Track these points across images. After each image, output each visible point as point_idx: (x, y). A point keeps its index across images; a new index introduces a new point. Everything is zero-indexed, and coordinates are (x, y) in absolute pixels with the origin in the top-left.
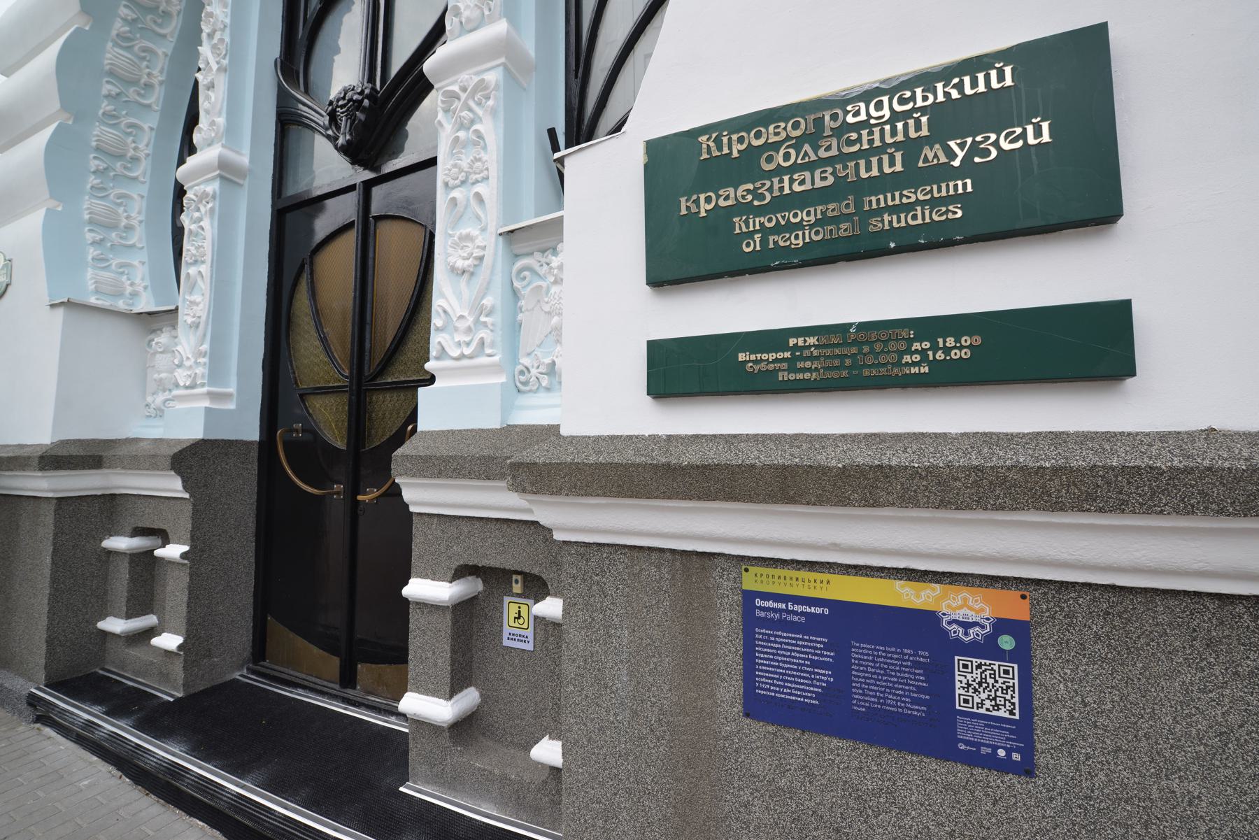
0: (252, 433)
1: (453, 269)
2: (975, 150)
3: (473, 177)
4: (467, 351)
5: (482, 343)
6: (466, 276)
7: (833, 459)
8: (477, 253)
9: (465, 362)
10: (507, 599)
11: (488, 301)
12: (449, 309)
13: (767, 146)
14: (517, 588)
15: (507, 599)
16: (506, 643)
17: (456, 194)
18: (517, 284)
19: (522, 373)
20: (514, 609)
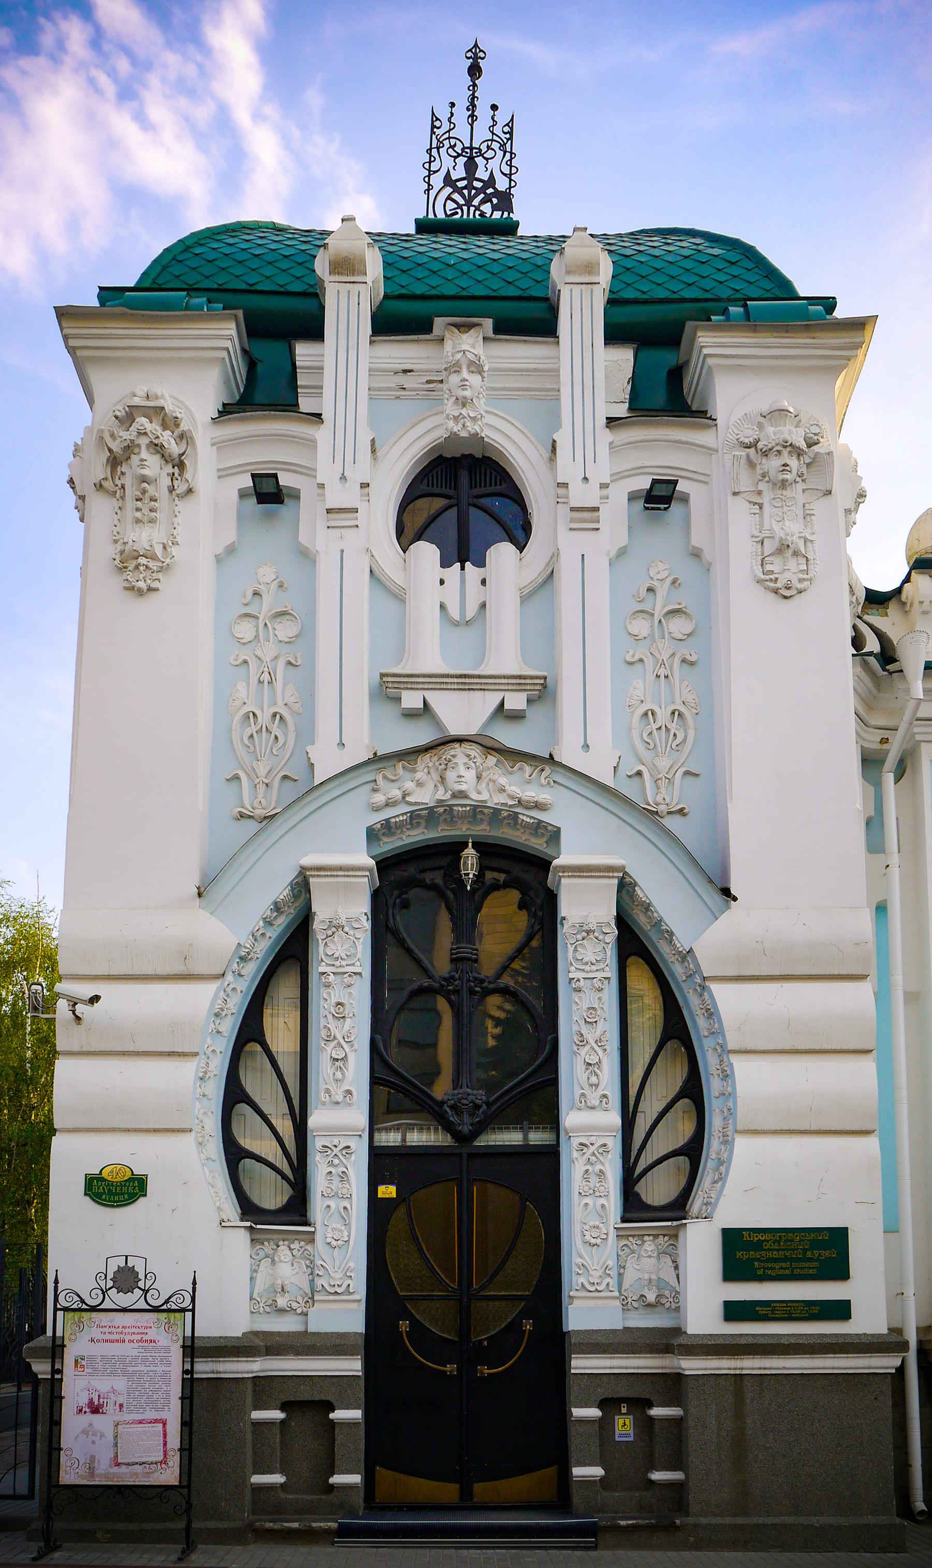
2: (820, 1255)
3: (597, 1194)
4: (599, 1288)
6: (595, 1247)
7: (784, 1341)
10: (617, 1417)
13: (765, 1240)
14: (624, 1410)
15: (617, 1417)
16: (617, 1439)
17: (586, 1200)
18: (620, 1253)
20: (621, 1422)
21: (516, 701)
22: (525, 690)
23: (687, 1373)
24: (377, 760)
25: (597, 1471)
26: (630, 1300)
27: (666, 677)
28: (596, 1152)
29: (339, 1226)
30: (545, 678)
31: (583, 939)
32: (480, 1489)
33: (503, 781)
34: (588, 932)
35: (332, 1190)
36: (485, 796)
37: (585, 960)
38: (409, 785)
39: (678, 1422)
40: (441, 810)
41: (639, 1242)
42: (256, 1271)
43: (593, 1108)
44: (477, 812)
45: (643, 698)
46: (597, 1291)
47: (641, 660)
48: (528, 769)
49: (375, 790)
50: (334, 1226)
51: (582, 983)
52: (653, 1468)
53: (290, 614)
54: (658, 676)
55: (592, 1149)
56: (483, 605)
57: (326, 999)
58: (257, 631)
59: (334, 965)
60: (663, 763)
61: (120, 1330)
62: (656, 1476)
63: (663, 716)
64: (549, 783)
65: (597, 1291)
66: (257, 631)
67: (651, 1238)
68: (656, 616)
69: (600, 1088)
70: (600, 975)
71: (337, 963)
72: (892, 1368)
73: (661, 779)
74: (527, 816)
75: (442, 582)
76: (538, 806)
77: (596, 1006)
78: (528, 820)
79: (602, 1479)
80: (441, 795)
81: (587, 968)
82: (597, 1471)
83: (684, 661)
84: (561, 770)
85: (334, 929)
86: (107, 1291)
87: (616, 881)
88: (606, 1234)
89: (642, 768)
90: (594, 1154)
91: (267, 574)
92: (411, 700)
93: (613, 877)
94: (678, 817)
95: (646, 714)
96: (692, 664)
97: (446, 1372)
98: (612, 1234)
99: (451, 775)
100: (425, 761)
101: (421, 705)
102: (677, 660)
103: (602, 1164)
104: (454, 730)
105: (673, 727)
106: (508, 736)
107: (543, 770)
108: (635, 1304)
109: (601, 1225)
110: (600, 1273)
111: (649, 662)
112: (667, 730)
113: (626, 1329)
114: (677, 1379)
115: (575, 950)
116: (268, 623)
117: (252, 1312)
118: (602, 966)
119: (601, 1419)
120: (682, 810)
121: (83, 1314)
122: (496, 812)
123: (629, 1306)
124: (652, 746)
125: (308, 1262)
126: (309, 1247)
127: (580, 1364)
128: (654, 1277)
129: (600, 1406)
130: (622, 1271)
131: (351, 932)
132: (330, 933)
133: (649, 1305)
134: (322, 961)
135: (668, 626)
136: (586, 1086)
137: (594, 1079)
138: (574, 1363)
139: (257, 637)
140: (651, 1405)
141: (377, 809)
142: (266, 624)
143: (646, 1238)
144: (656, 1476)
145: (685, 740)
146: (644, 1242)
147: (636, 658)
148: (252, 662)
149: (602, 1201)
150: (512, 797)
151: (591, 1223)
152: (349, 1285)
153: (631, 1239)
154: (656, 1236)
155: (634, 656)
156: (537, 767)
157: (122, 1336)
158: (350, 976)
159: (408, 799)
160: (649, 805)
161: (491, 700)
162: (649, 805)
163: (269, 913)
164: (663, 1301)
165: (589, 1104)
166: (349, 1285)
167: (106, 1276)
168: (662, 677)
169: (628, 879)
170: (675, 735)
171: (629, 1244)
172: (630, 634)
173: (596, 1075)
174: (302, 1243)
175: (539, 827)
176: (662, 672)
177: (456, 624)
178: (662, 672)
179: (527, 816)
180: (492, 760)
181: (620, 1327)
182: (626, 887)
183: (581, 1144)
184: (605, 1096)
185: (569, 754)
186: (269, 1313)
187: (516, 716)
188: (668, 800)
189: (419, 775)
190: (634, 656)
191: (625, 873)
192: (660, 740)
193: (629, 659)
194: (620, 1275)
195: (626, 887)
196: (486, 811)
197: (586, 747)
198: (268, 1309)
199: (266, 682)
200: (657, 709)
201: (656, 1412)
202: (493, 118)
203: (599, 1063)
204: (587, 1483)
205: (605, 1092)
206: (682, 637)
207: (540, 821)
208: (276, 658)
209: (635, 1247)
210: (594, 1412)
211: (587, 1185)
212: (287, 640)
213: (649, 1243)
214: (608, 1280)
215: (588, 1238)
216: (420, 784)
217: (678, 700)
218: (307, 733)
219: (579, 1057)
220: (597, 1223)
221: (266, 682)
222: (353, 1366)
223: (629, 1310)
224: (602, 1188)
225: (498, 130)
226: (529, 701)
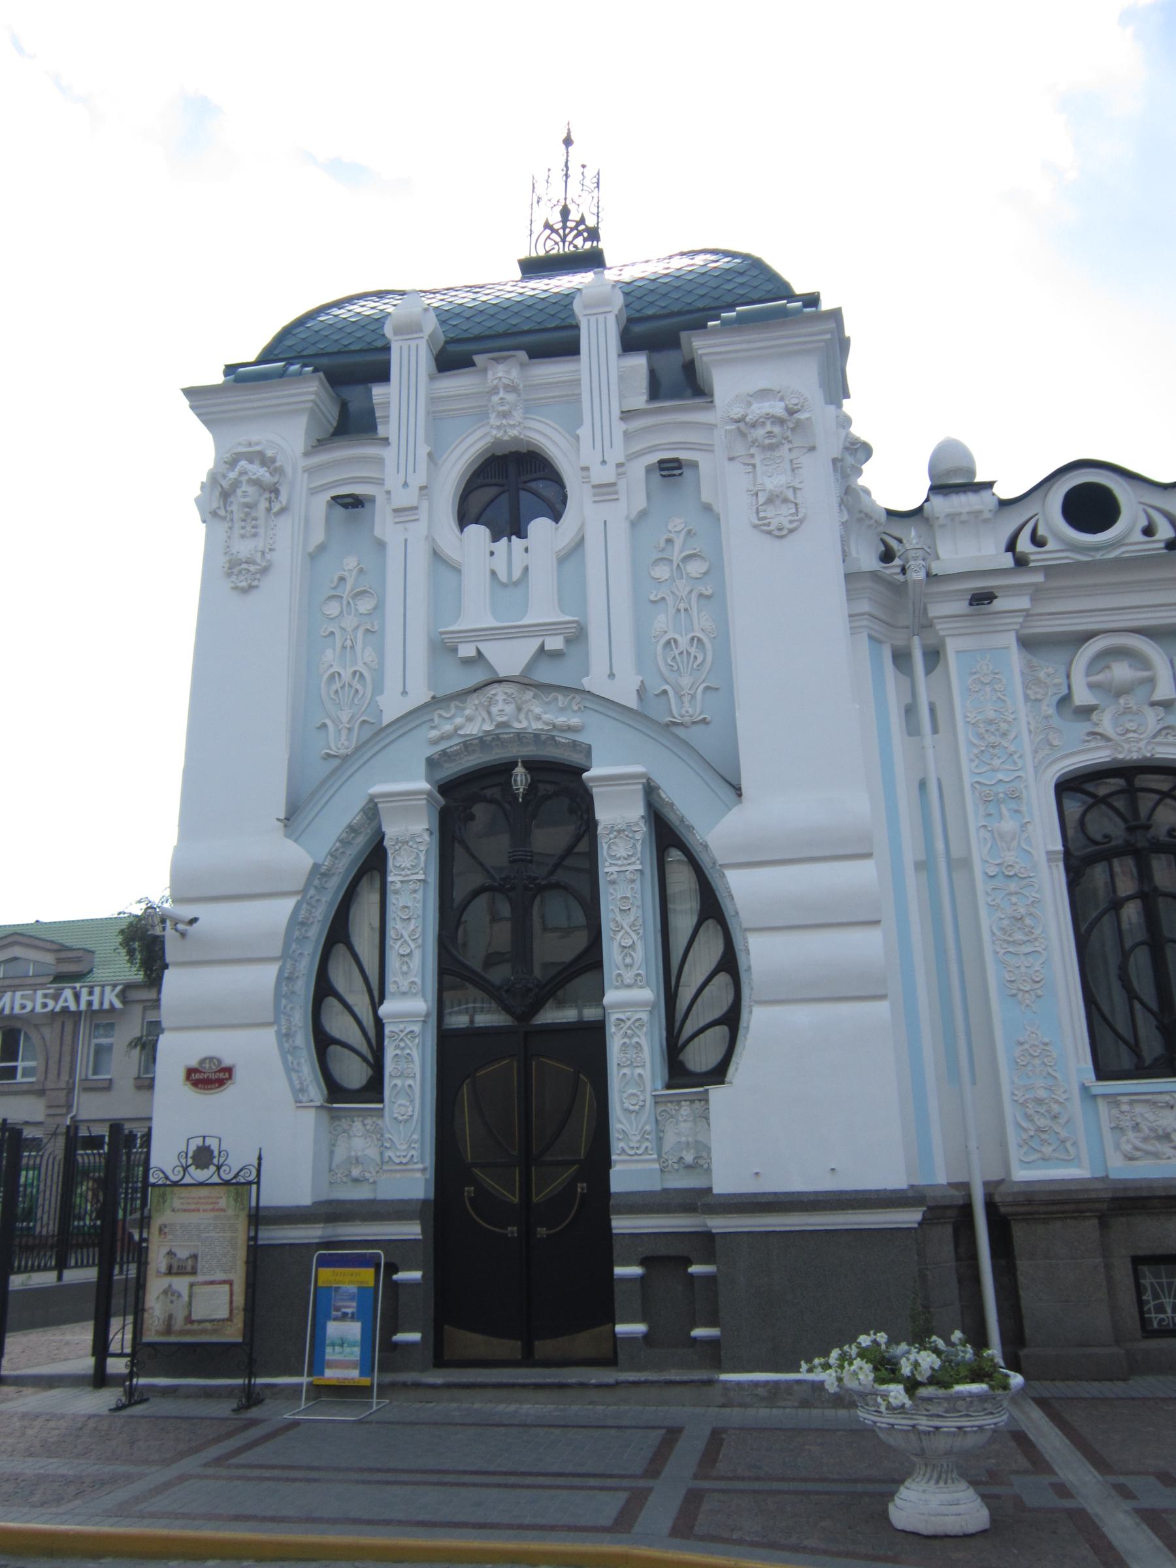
0: (432, 1196)
1: (626, 1110)
3: (635, 1064)
4: (639, 1152)
5: (647, 1148)
6: (634, 1114)
8: (641, 1103)
9: (636, 1158)
11: (648, 1128)
12: (625, 1129)
17: (625, 1070)
18: (659, 1118)
19: (664, 1162)
21: (555, 643)
22: (561, 634)
23: (714, 1231)
24: (435, 702)
25: (639, 1328)
26: (670, 1162)
27: (686, 610)
28: (632, 1026)
29: (403, 1102)
30: (576, 622)
31: (615, 838)
32: (544, 1347)
33: (537, 710)
34: (619, 831)
35: (398, 1070)
36: (524, 724)
37: (618, 855)
38: (459, 720)
39: (710, 1279)
40: (489, 738)
41: (677, 1108)
42: (334, 1145)
43: (629, 986)
44: (520, 736)
45: (666, 629)
46: (636, 1154)
47: (663, 599)
48: (560, 697)
49: (433, 728)
50: (399, 1102)
51: (615, 876)
52: (694, 1325)
53: (368, 592)
54: (678, 610)
55: (629, 1023)
56: (526, 569)
57: (394, 904)
58: (342, 608)
59: (400, 875)
60: (686, 681)
61: (195, 1201)
62: (698, 1332)
63: (683, 641)
64: (580, 708)
65: (636, 1154)
66: (342, 608)
67: (688, 1103)
68: (674, 560)
69: (636, 966)
70: (631, 868)
71: (403, 873)
72: (914, 1222)
73: (684, 695)
74: (563, 738)
75: (492, 554)
76: (570, 729)
77: (629, 895)
78: (563, 741)
79: (646, 1337)
80: (488, 727)
81: (619, 862)
82: (639, 1328)
83: (701, 595)
84: (588, 697)
85: (400, 844)
86: (188, 1167)
87: (641, 787)
88: (644, 1101)
89: (667, 687)
90: (630, 1028)
91: (351, 563)
92: (466, 651)
93: (639, 783)
94: (701, 727)
95: (668, 643)
96: (708, 597)
97: (507, 1234)
98: (649, 1101)
99: (494, 710)
100: (475, 700)
101: (473, 653)
102: (694, 596)
103: (639, 1036)
104: (502, 674)
105: (693, 650)
106: (545, 674)
107: (574, 698)
108: (676, 1166)
109: (639, 1093)
110: (638, 1138)
111: (670, 600)
112: (689, 653)
113: (665, 1191)
114: (708, 1237)
115: (609, 847)
116: (351, 602)
117: (331, 1183)
118: (633, 859)
119: (643, 1278)
120: (704, 719)
121: (167, 1188)
122: (536, 736)
123: (670, 1168)
124: (675, 668)
125: (378, 1136)
126: (379, 1122)
127: (621, 1224)
128: (690, 1139)
129: (643, 1262)
130: (662, 1135)
131: (415, 846)
132: (397, 847)
133: (689, 1167)
134: (392, 872)
135: (685, 568)
136: (622, 967)
137: (628, 960)
138: (614, 1223)
139: (342, 612)
140: (690, 1262)
141: (435, 742)
142: (349, 603)
143: (683, 1103)
144: (698, 1332)
145: (704, 661)
146: (681, 1107)
147: (659, 597)
148: (338, 633)
149: (639, 1071)
150: (547, 724)
151: (630, 1091)
152: (413, 1156)
153: (669, 1104)
154: (692, 1101)
155: (656, 595)
156: (568, 696)
157: (197, 1206)
158: (414, 882)
159: (461, 732)
160: (675, 718)
161: (533, 645)
162: (675, 718)
163: (344, 835)
164: (701, 1162)
165: (625, 983)
166: (413, 1156)
167: (187, 1154)
168: (682, 611)
169: (652, 784)
170: (696, 657)
171: (668, 1109)
172: (653, 578)
173: (630, 954)
174: (375, 1119)
175: (574, 745)
176: (682, 606)
177: (504, 585)
178: (682, 606)
179: (563, 738)
180: (529, 694)
181: (658, 1187)
182: (650, 791)
183: (618, 1019)
184: (639, 975)
185: (596, 682)
186: (345, 1183)
187: (556, 655)
188: (691, 711)
189: (467, 712)
190: (656, 595)
191: (649, 779)
192: (682, 662)
193: (652, 598)
194: (660, 1140)
195: (650, 791)
196: (527, 735)
197: (612, 676)
198: (345, 1179)
199: (348, 648)
200: (677, 637)
201: (694, 1269)
202: (583, 173)
203: (633, 946)
204: (631, 1340)
205: (639, 972)
206: (699, 576)
207: (574, 741)
208: (357, 627)
209: (674, 1112)
210: (636, 1270)
211: (625, 1057)
212: (366, 612)
213: (686, 1108)
214: (647, 1144)
215: (626, 1105)
216: (470, 719)
217: (696, 627)
218: (378, 688)
219: (615, 942)
220: (635, 1091)
221: (348, 648)
222: (412, 1230)
223: (670, 1172)
224: (639, 1059)
225: (586, 182)
226: (568, 641)
